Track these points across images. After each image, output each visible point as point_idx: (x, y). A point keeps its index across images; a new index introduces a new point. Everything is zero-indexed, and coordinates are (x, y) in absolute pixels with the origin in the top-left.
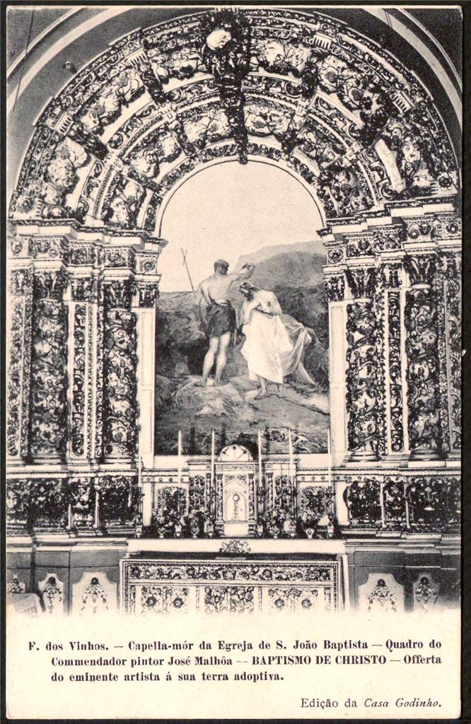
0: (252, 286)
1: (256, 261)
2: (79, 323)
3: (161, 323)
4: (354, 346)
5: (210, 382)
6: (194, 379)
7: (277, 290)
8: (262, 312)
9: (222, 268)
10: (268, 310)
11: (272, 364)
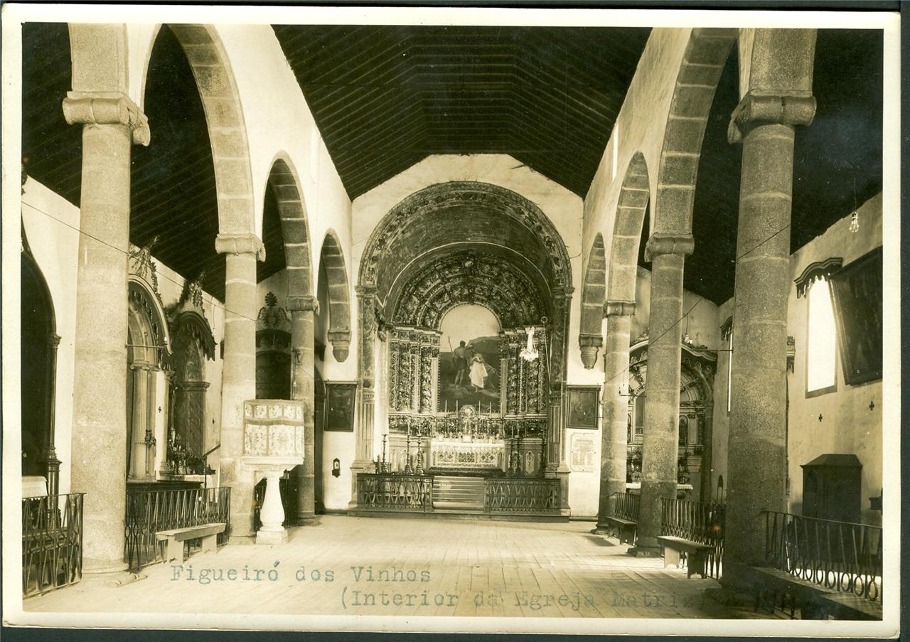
1: (475, 342)
3: (441, 365)
4: (510, 375)
6: (452, 385)
7: (483, 353)
9: (463, 343)
11: (480, 381)
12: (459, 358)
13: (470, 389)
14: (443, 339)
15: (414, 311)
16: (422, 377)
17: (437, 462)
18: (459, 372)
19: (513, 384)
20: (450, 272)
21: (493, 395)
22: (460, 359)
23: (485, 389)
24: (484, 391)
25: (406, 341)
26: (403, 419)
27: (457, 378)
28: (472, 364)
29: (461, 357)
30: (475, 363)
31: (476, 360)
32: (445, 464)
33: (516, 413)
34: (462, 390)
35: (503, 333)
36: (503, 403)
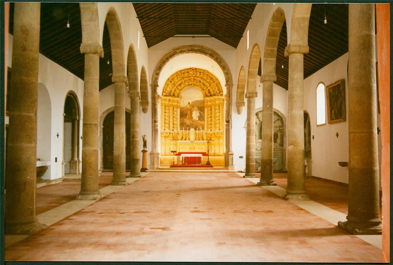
4: (208, 115)
5: (188, 120)
6: (185, 120)
7: (197, 106)
9: (189, 103)
12: (188, 109)
14: (182, 102)
18: (188, 114)
19: (210, 119)
22: (188, 109)
27: (187, 116)
28: (193, 111)
29: (189, 108)
30: (194, 111)
31: (195, 109)
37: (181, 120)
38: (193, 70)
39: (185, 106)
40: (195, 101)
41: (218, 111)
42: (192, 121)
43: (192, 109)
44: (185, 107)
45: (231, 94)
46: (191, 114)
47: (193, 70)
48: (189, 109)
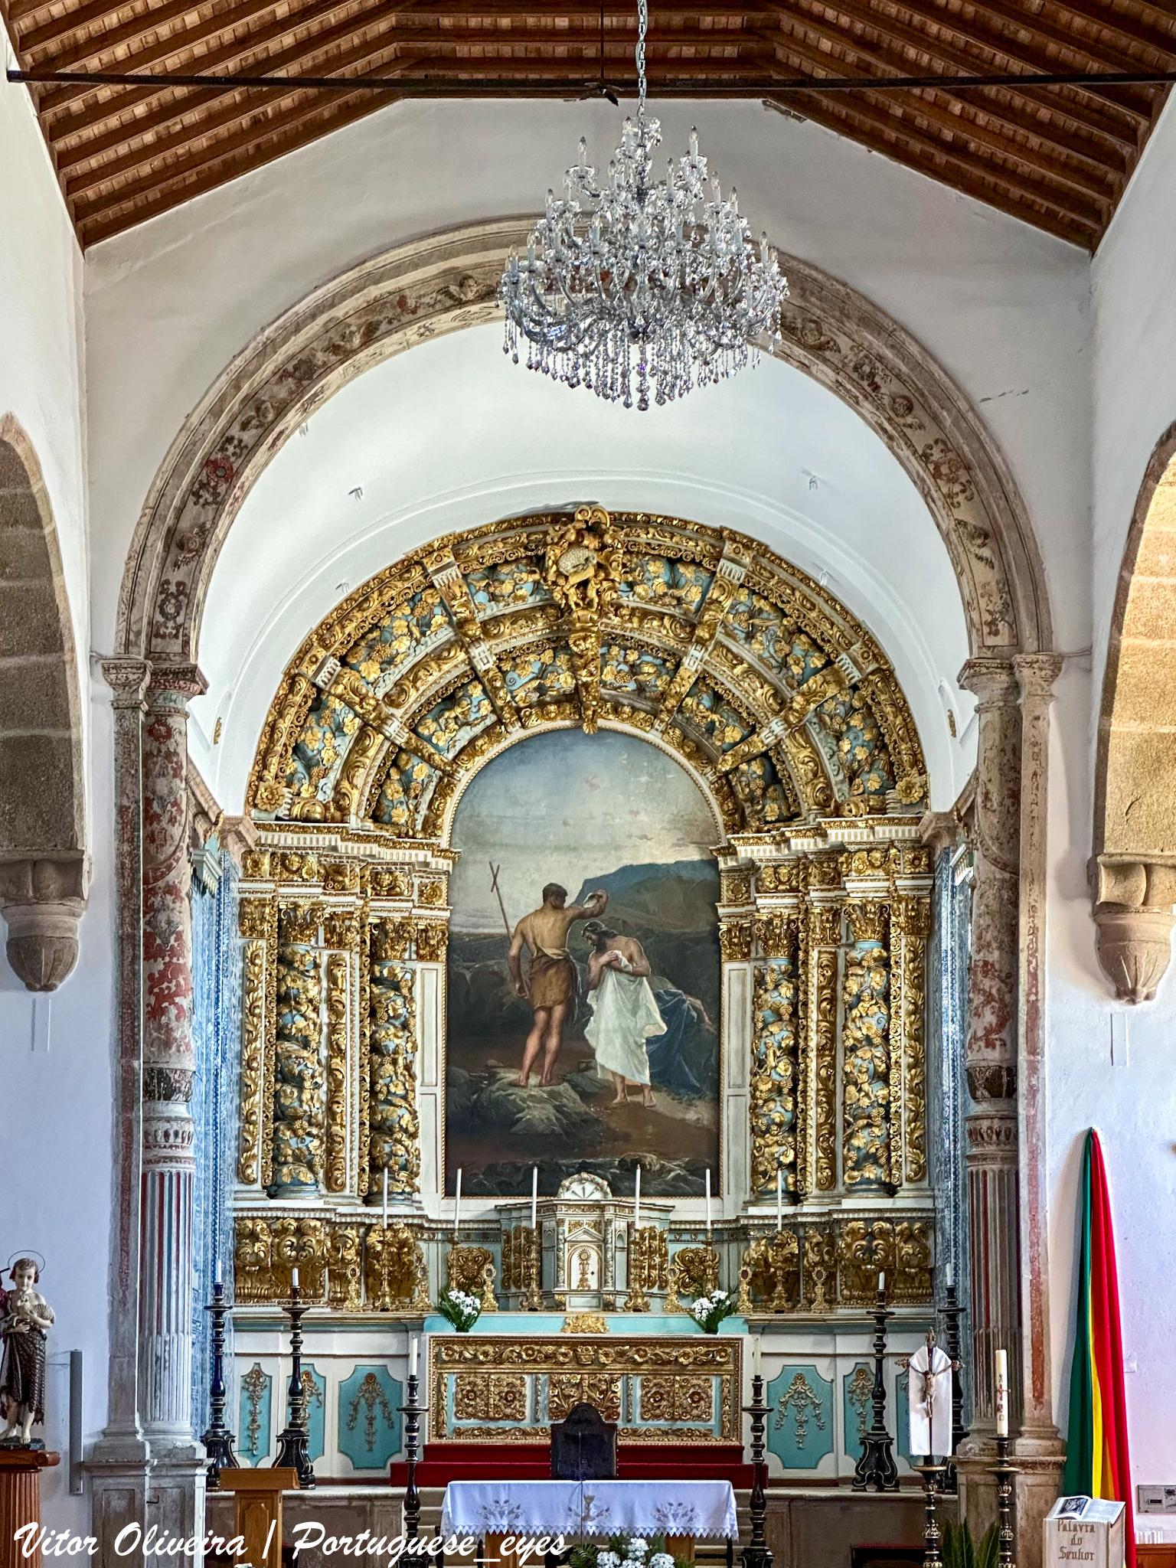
0: (604, 928)
2: (335, 983)
6: (511, 1076)
7: (643, 935)
8: (619, 970)
9: (554, 895)
10: (630, 968)
11: (631, 1051)
13: (591, 1089)
15: (339, 763)
16: (376, 1048)
17: (452, 1421)
18: (541, 1016)
20: (493, 598)
21: (697, 1114)
23: (653, 1088)
24: (658, 1101)
25: (305, 894)
26: (300, 1232)
27: (532, 1044)
28: (597, 985)
29: (549, 952)
30: (611, 980)
31: (612, 966)
32: (488, 1433)
33: (795, 1197)
34: (551, 1094)
35: (730, 851)
36: (735, 1152)
37: (462, 1073)
38: (595, 529)
39: (513, 924)
40: (626, 870)
41: (876, 980)
42: (584, 1096)
43: (584, 959)
44: (505, 941)
45: (1027, 768)
46: (577, 1015)
47: (595, 529)
48: (552, 963)
